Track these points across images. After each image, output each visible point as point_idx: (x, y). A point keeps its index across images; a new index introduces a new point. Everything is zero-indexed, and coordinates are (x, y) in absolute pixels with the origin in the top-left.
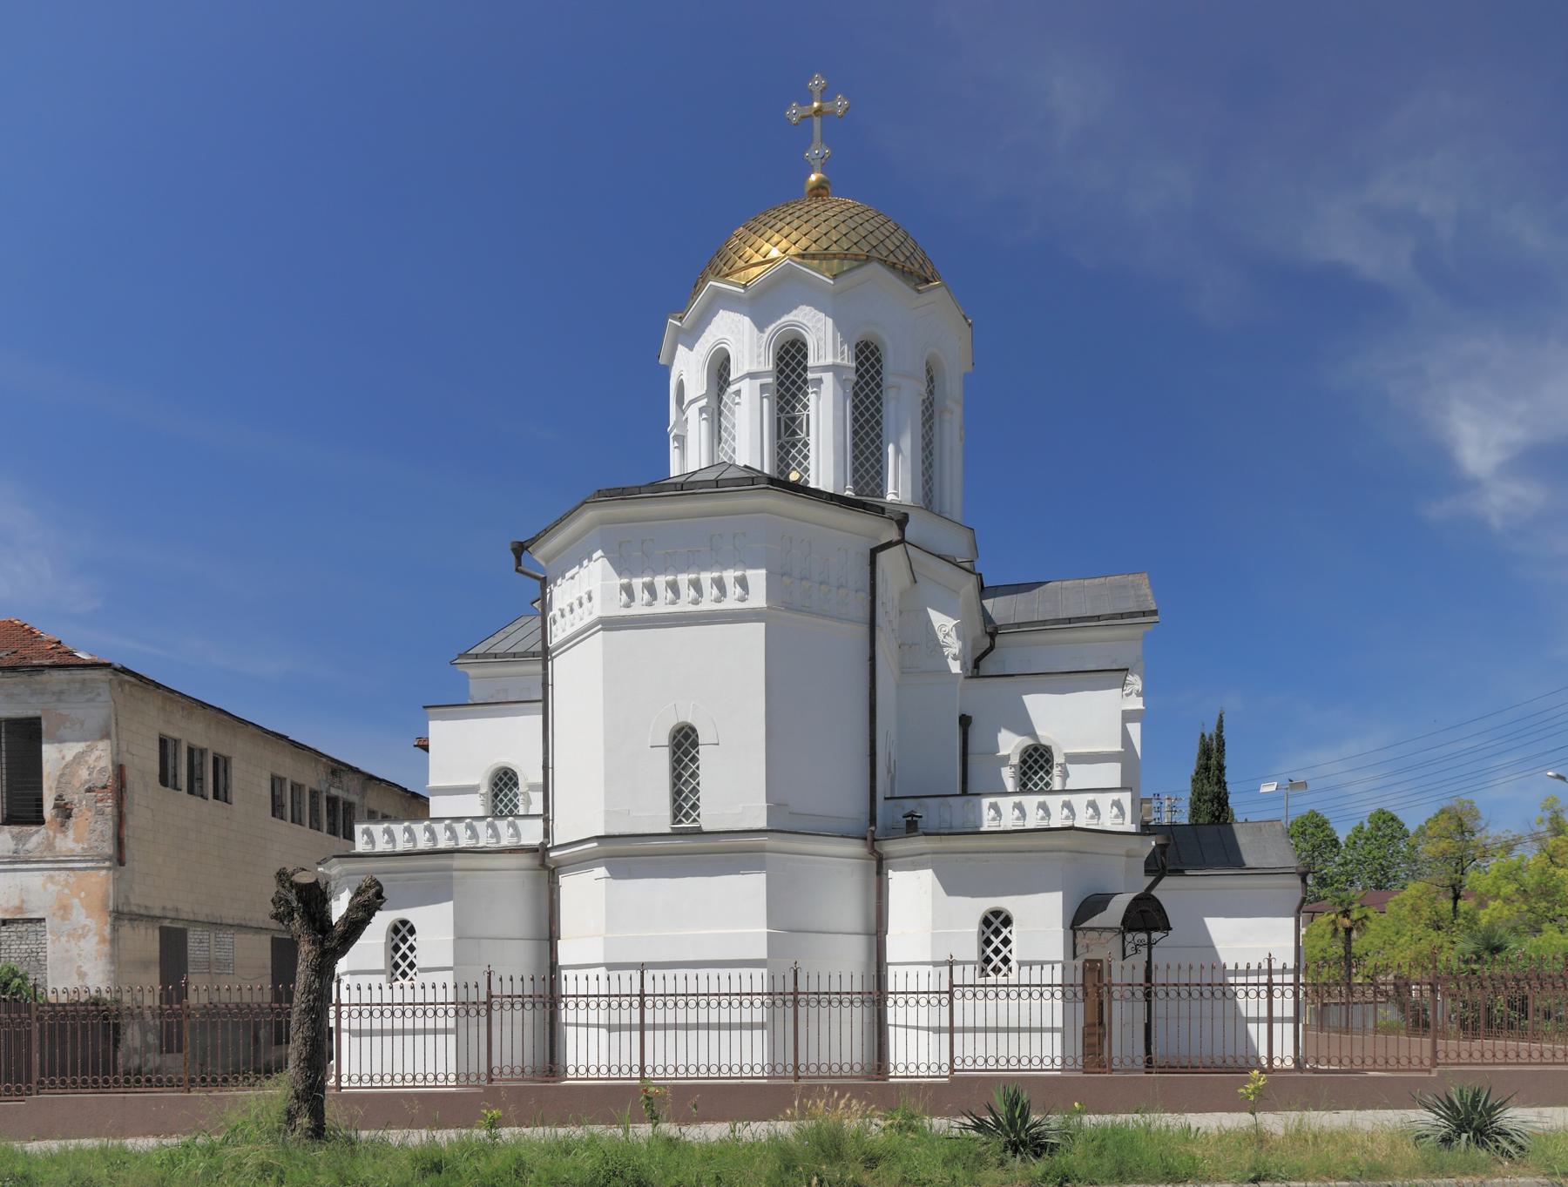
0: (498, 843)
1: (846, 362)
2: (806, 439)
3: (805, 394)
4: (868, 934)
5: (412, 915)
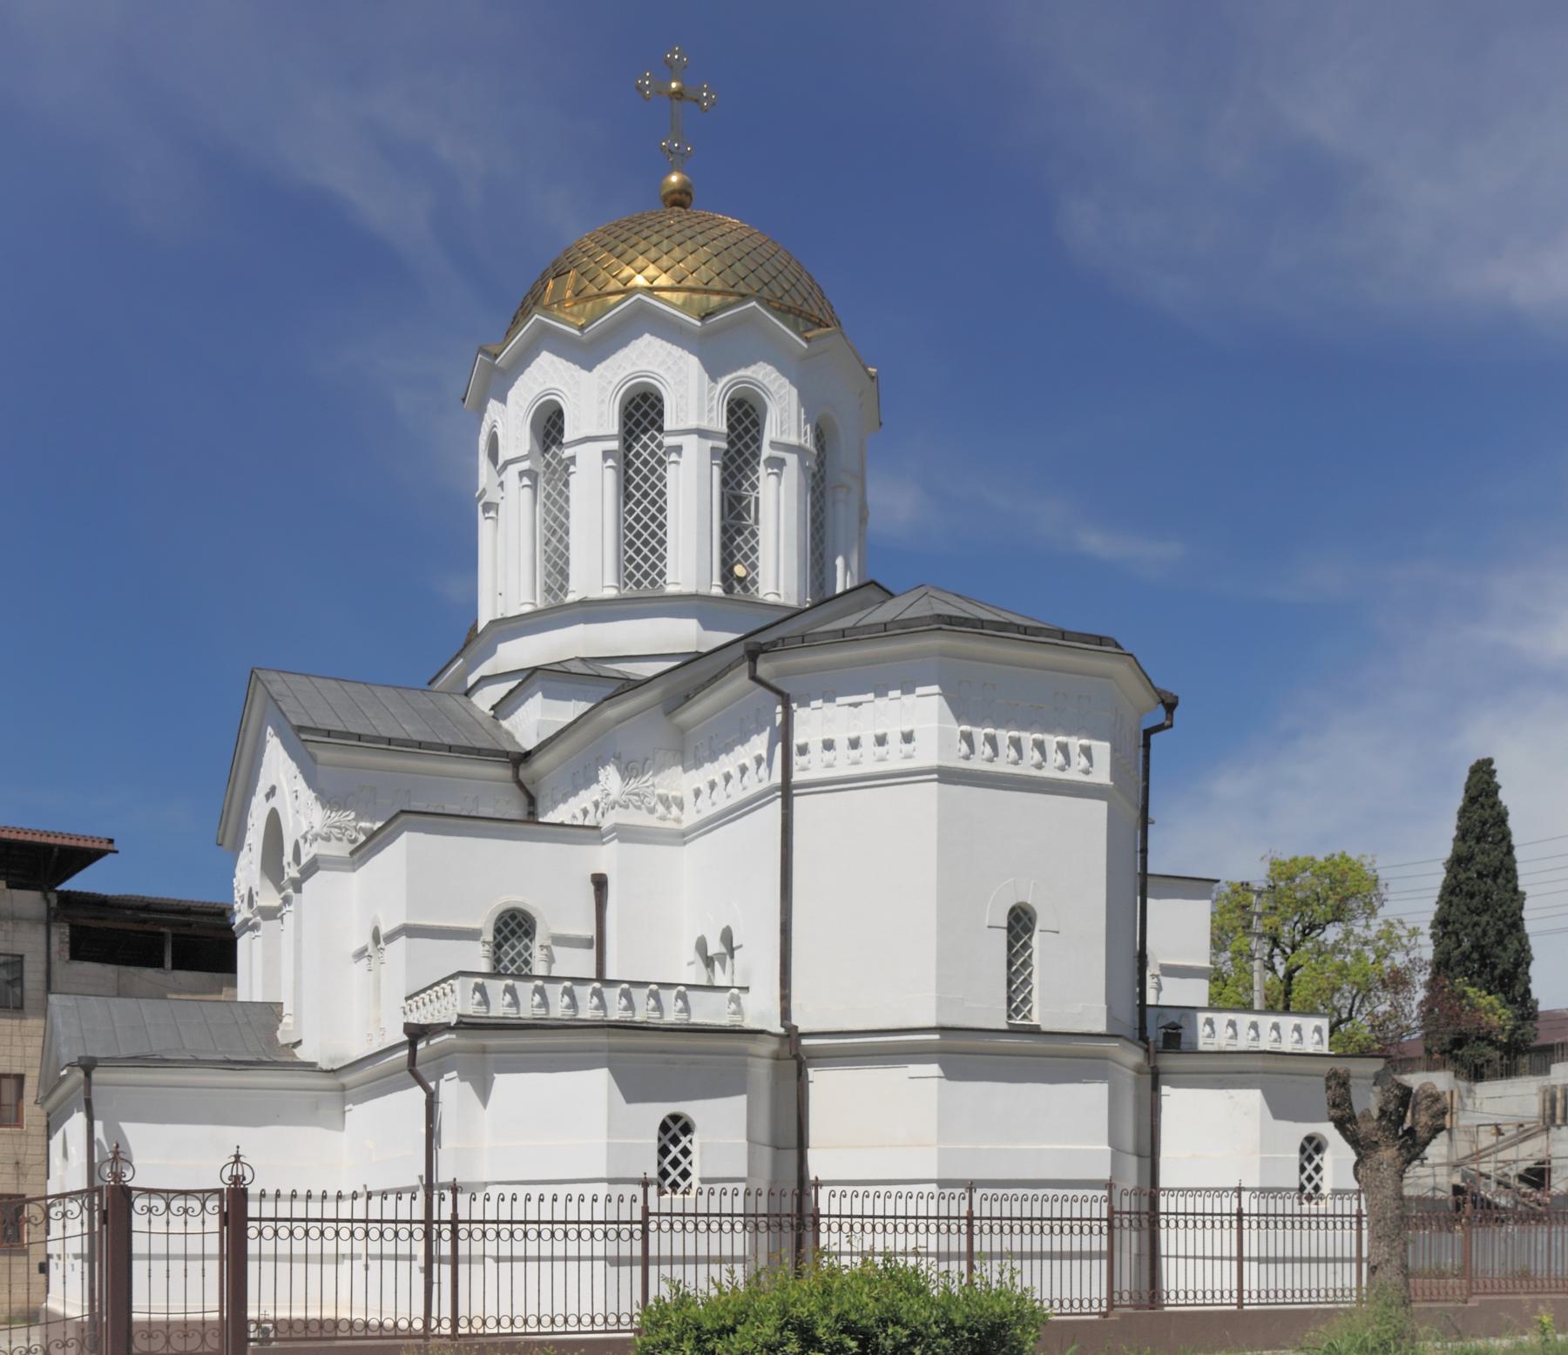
0: (661, 1017)
1: (808, 445)
2: (755, 527)
3: (755, 471)
4: (1139, 1155)
5: (688, 1108)
